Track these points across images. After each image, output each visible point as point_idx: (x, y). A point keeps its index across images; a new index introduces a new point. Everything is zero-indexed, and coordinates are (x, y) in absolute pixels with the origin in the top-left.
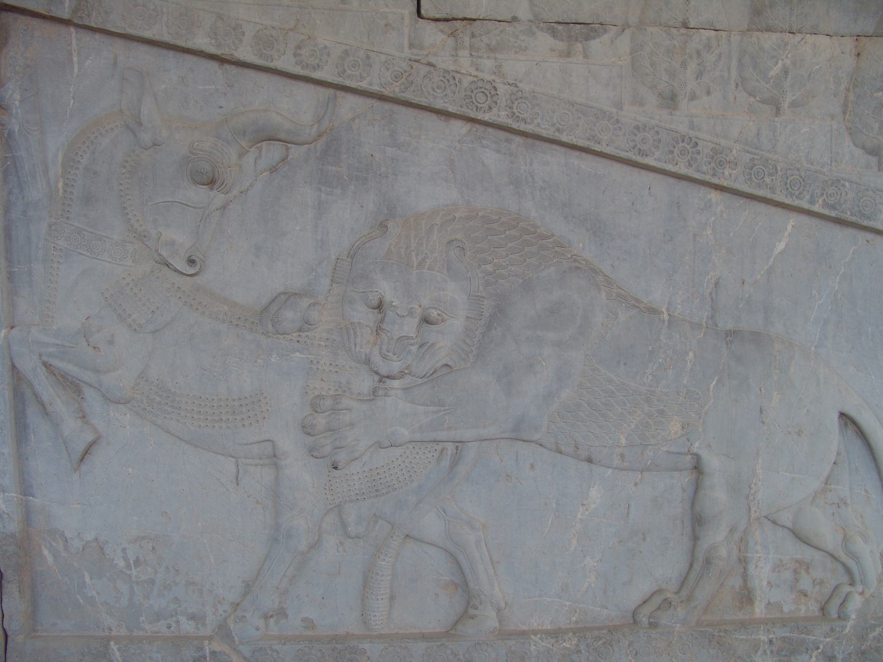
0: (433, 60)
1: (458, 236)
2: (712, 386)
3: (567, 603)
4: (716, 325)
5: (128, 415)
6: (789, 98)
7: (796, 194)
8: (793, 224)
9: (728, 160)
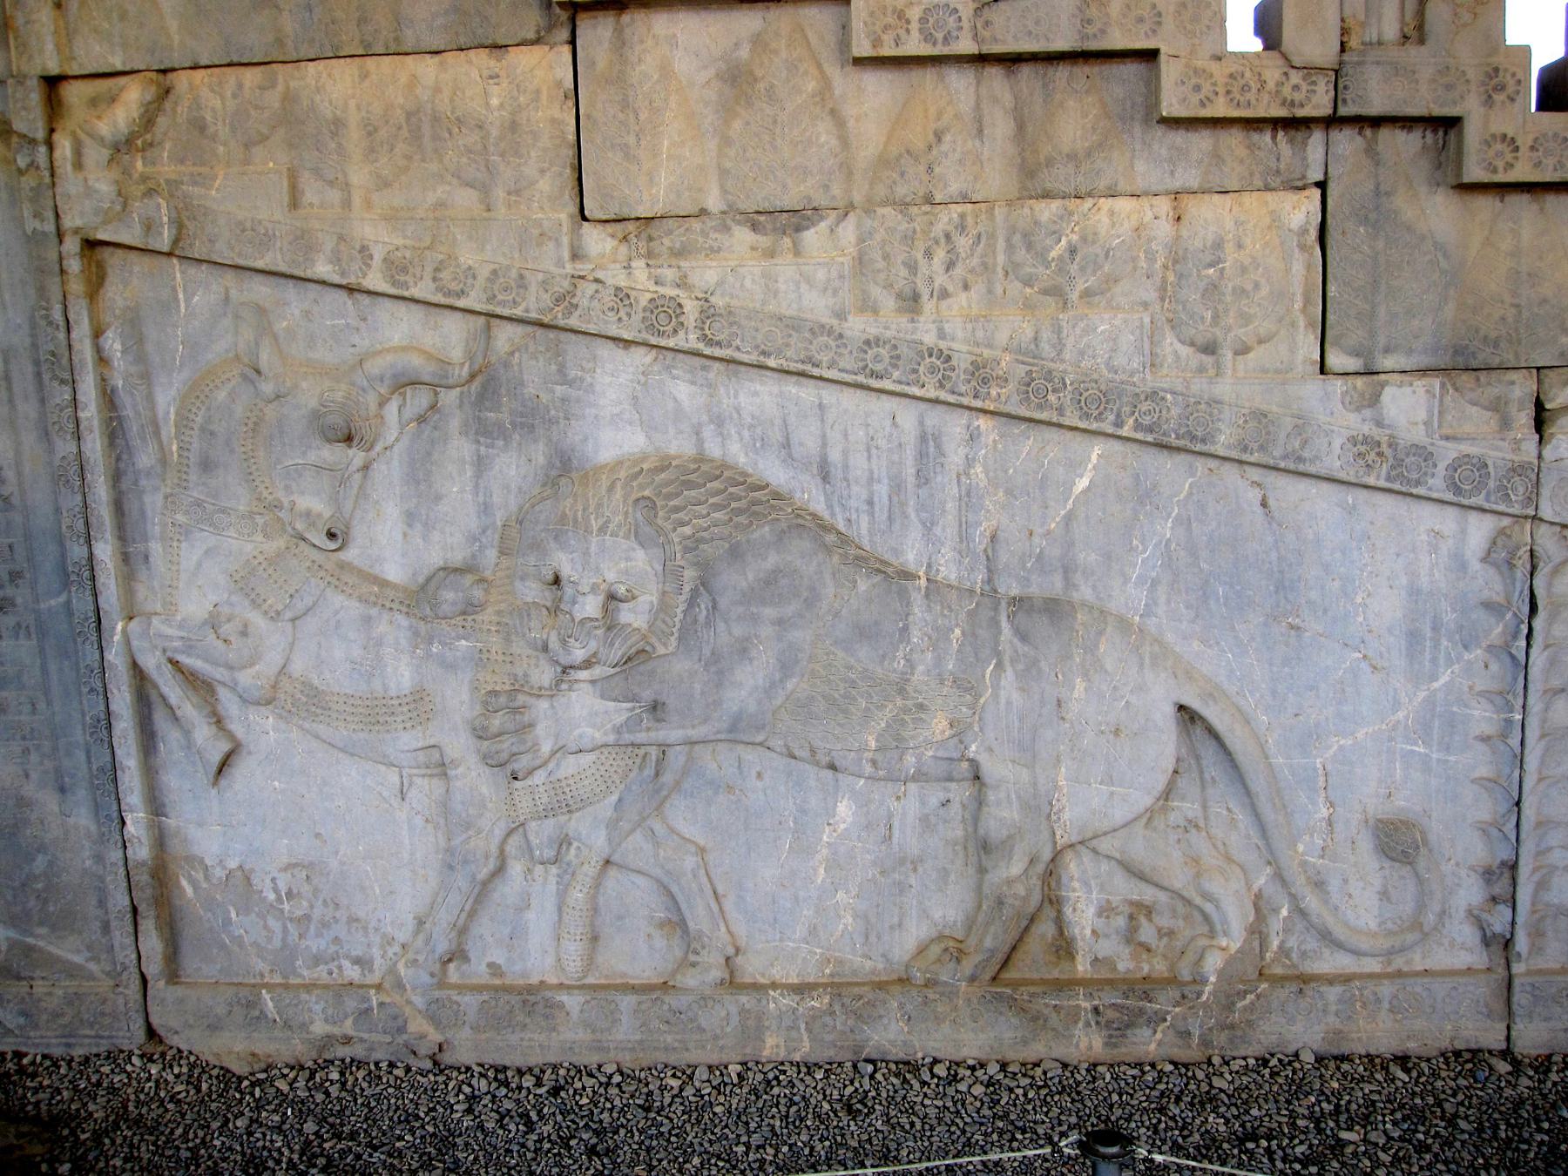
0: (600, 275)
1: (647, 493)
2: (988, 671)
3: (818, 951)
4: (996, 591)
5: (271, 719)
6: (1081, 286)
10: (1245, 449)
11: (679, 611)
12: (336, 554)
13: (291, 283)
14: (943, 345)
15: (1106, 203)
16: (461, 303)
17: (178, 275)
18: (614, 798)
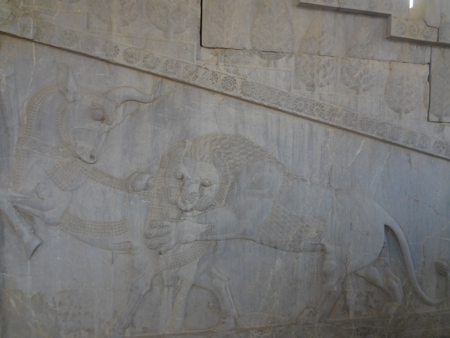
0: (207, 66)
1: (218, 147)
4: (331, 187)
5: (58, 231)
7: (366, 129)
8: (364, 142)
9: (336, 114)
10: (407, 143)
11: (227, 190)
12: (92, 165)
13: (82, 58)
14: (321, 102)
15: (371, 61)
16: (153, 71)
17: (34, 50)
18: (197, 261)
